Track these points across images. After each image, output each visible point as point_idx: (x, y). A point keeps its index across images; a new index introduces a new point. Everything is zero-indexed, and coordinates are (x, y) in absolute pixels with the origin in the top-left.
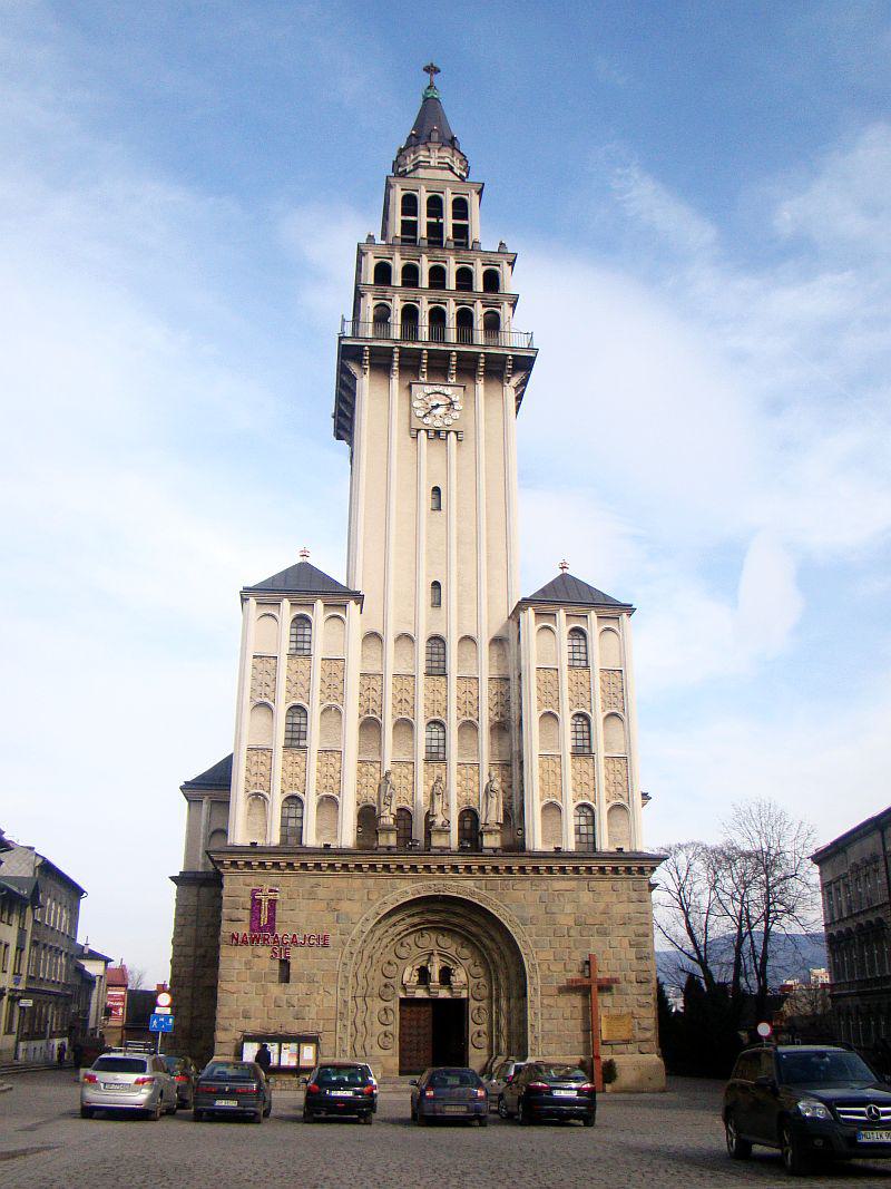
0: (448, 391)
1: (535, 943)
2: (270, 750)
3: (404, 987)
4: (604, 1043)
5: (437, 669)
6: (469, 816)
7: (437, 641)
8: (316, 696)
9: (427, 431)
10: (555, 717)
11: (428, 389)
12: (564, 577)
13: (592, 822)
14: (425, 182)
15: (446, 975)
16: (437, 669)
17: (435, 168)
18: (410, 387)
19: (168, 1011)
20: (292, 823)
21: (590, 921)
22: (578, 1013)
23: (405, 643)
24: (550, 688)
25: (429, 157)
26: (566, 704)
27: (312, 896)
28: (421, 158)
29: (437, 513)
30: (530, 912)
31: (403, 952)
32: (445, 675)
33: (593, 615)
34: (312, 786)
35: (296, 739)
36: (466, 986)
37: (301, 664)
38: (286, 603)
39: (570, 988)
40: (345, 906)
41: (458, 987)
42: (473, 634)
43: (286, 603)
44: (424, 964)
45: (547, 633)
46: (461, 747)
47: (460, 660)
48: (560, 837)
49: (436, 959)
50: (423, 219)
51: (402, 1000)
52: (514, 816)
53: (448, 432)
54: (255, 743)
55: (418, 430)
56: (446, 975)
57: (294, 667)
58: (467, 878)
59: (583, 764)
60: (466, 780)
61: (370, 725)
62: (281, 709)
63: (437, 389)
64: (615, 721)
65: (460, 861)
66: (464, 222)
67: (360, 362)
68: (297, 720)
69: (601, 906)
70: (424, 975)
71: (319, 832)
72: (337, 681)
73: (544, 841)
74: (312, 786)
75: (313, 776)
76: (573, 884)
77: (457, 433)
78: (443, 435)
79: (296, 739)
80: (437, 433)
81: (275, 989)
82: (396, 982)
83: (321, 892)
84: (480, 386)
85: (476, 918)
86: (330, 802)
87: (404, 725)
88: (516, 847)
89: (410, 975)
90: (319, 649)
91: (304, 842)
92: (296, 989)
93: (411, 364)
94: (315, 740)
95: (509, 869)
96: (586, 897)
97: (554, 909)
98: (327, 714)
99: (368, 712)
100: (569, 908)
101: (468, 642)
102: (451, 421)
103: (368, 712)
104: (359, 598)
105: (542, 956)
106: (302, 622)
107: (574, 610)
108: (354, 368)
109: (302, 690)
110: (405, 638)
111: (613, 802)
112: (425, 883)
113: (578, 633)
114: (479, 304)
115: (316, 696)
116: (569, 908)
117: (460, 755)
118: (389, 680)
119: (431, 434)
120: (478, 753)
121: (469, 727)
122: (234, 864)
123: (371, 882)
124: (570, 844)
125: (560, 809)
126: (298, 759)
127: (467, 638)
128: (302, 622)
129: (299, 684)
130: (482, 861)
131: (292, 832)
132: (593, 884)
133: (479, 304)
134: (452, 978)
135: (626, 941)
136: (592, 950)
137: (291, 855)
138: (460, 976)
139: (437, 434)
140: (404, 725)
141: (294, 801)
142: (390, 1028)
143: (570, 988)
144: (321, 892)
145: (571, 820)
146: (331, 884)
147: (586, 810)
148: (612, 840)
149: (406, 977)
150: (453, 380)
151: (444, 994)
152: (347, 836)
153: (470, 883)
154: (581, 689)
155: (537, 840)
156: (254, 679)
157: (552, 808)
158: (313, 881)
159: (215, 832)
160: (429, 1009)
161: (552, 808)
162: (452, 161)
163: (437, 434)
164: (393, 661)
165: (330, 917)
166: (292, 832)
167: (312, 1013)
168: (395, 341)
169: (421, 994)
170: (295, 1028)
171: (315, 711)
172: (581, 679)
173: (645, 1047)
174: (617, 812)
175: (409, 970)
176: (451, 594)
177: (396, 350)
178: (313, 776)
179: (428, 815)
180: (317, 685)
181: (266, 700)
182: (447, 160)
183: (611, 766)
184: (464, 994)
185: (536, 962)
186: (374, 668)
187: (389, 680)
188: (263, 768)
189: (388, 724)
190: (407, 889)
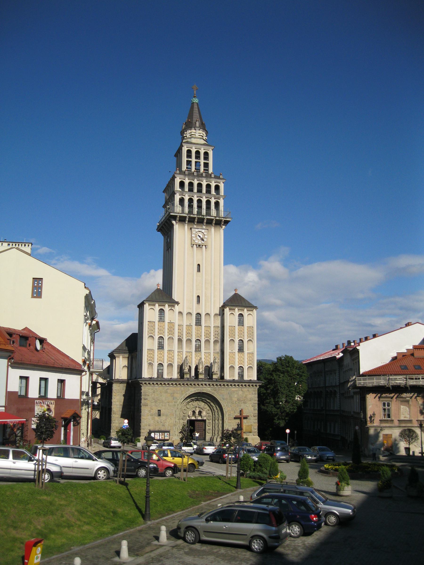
0: (203, 231)
1: (227, 405)
5: (198, 322)
7: (199, 314)
8: (166, 334)
9: (196, 245)
10: (234, 340)
11: (197, 230)
12: (235, 294)
13: (243, 371)
14: (194, 145)
15: (200, 413)
16: (198, 322)
17: (198, 138)
18: (191, 229)
19: (127, 424)
20: (160, 371)
21: (241, 399)
23: (189, 315)
24: (232, 332)
25: (195, 133)
26: (237, 336)
27: (166, 392)
28: (193, 133)
29: (199, 273)
31: (188, 406)
32: (201, 325)
33: (245, 310)
34: (166, 360)
35: (161, 347)
36: (205, 416)
37: (162, 324)
38: (157, 305)
40: (176, 395)
42: (209, 313)
43: (157, 305)
44: (194, 410)
45: (232, 315)
46: (205, 347)
47: (205, 321)
48: (234, 376)
53: (203, 245)
54: (149, 348)
56: (200, 413)
57: (160, 325)
59: (241, 355)
64: (250, 342)
65: (207, 383)
66: (207, 162)
68: (160, 341)
69: (244, 395)
70: (194, 412)
71: (168, 374)
73: (230, 377)
74: (166, 360)
75: (166, 358)
76: (237, 389)
77: (205, 246)
78: (201, 246)
79: (161, 347)
80: (199, 245)
81: (157, 418)
82: (186, 415)
83: (169, 391)
86: (170, 365)
87: (189, 341)
88: (222, 377)
89: (190, 413)
90: (167, 320)
91: (164, 377)
92: (163, 418)
93: (192, 220)
95: (220, 385)
96: (240, 393)
98: (169, 339)
100: (236, 396)
101: (208, 315)
104: (178, 303)
105: (228, 409)
106: (162, 311)
107: (240, 308)
108: (174, 222)
110: (189, 314)
111: (249, 366)
113: (241, 315)
114: (213, 198)
116: (236, 396)
117: (205, 350)
118: (185, 327)
119: (198, 246)
120: (209, 349)
121: (207, 341)
122: (145, 383)
123: (182, 388)
124: (236, 378)
125: (234, 368)
126: (161, 352)
127: (207, 314)
128: (162, 311)
129: (161, 330)
130: (213, 383)
131: (160, 374)
133: (213, 198)
135: (251, 406)
136: (242, 407)
137: (160, 380)
138: (204, 413)
140: (189, 341)
141: (161, 365)
144: (169, 391)
145: (237, 371)
146: (171, 389)
147: (241, 368)
148: (248, 376)
149: (189, 414)
151: (200, 418)
152: (175, 375)
153: (209, 389)
155: (227, 377)
156: (148, 328)
157: (232, 367)
158: (166, 388)
161: (232, 367)
164: (185, 321)
166: (160, 374)
167: (167, 424)
169: (193, 418)
170: (163, 429)
171: (166, 338)
172: (241, 329)
173: (255, 434)
175: (190, 412)
176: (202, 299)
178: (166, 358)
180: (166, 331)
181: (152, 335)
182: (202, 135)
183: (249, 355)
184: (205, 418)
185: (227, 411)
186: (181, 323)
187: (185, 327)
188: (151, 355)
190: (192, 390)
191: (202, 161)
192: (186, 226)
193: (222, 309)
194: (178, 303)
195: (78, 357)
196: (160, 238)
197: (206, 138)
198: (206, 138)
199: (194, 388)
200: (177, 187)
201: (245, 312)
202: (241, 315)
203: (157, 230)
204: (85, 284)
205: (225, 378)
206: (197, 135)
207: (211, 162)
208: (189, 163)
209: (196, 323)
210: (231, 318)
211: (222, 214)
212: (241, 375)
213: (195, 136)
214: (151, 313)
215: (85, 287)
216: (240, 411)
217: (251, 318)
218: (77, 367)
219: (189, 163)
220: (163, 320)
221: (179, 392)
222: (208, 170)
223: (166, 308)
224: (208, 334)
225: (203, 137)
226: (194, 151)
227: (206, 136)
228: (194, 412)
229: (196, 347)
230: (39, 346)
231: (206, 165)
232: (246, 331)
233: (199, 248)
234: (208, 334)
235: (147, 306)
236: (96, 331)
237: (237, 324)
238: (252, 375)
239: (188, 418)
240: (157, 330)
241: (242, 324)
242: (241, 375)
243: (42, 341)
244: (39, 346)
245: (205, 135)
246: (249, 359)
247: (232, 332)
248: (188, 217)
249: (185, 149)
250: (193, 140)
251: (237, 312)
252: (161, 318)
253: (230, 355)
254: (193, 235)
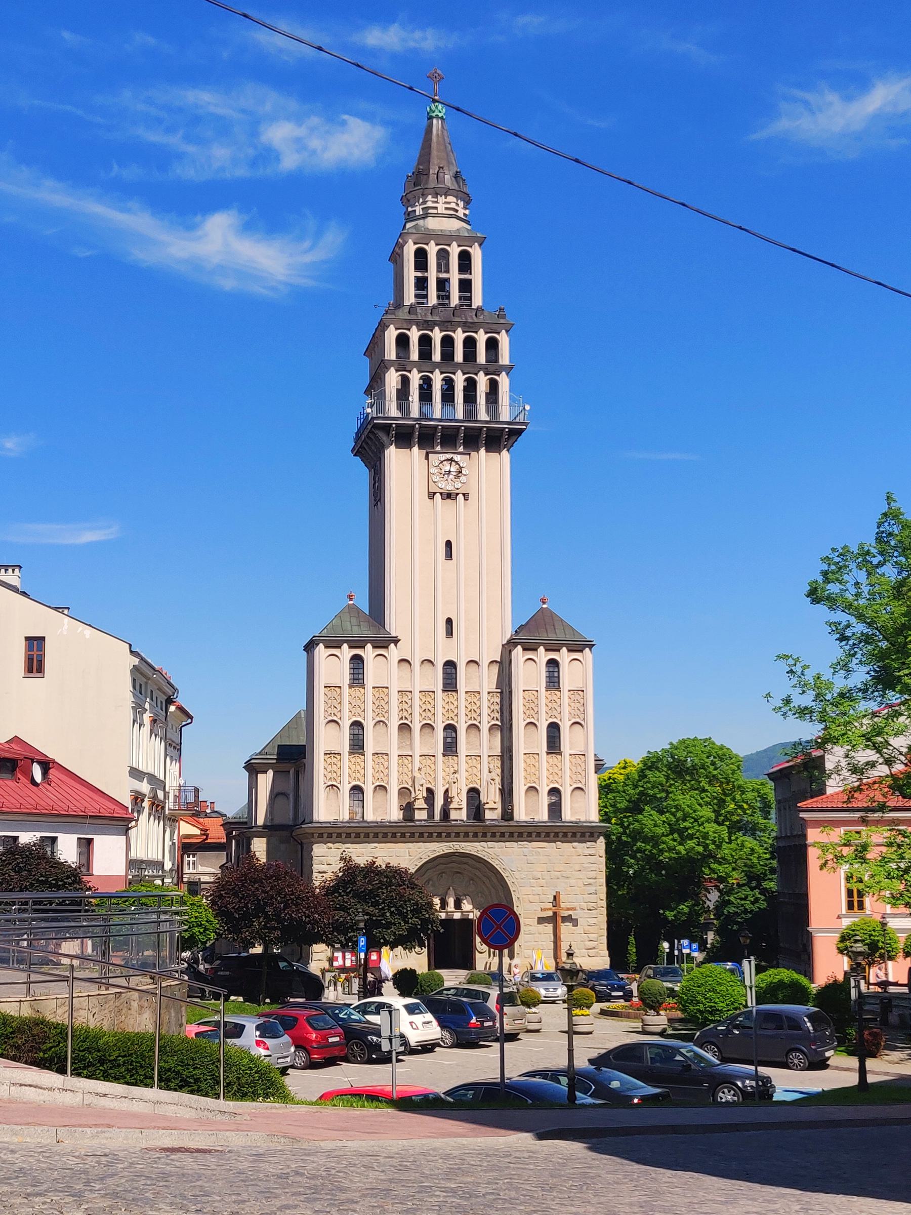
0: (457, 458)
2: (339, 754)
5: (450, 684)
6: (474, 793)
7: (450, 665)
8: (370, 714)
9: (441, 494)
10: (535, 725)
11: (443, 457)
16: (450, 684)
24: (532, 705)
25: (437, 202)
28: (430, 204)
32: (456, 691)
35: (357, 746)
37: (358, 691)
46: (467, 743)
50: (432, 274)
52: (507, 792)
53: (457, 494)
54: (329, 749)
55: (435, 493)
60: (472, 770)
61: (404, 728)
62: (346, 724)
63: (449, 456)
67: (388, 433)
68: (356, 732)
71: (375, 810)
72: (383, 703)
75: (370, 772)
77: (464, 495)
79: (357, 746)
84: (483, 451)
87: (428, 727)
88: (507, 814)
94: (370, 745)
98: (378, 727)
99: (402, 718)
102: (460, 485)
103: (402, 718)
104: (396, 641)
106: (357, 661)
109: (359, 710)
111: (575, 786)
113: (553, 663)
115: (370, 714)
118: (417, 695)
128: (357, 661)
139: (449, 496)
140: (428, 727)
145: (544, 800)
148: (573, 813)
150: (461, 449)
151: (457, 916)
154: (555, 705)
155: (521, 814)
159: (278, 794)
162: (457, 205)
163: (449, 496)
168: (416, 419)
171: (369, 725)
172: (555, 698)
174: (578, 792)
177: (417, 426)
178: (370, 772)
179: (447, 791)
180: (370, 707)
182: (453, 205)
187: (417, 695)
189: (416, 727)
191: (455, 277)
192: (416, 449)
193: (510, 645)
194: (396, 641)
195: (121, 790)
196: (361, 471)
197: (467, 212)
198: (467, 212)
200: (391, 352)
201: (564, 656)
202: (553, 663)
203: (352, 451)
204: (130, 645)
205: (516, 817)
206: (441, 209)
207: (477, 276)
208: (421, 283)
209: (445, 685)
210: (528, 671)
211: (505, 415)
212: (555, 809)
213: (435, 211)
214: (332, 666)
215: (131, 652)
216: (555, 897)
217: (576, 670)
218: (120, 813)
219: (421, 283)
220: (361, 681)
222: (470, 298)
223: (368, 653)
224: (474, 711)
225: (457, 211)
226: (432, 250)
227: (465, 208)
229: (445, 743)
230: (38, 777)
231: (465, 286)
232: (566, 700)
233: (448, 500)
234: (474, 711)
235: (321, 651)
236: (184, 723)
237: (544, 684)
238: (584, 809)
240: (346, 707)
241: (556, 684)
242: (555, 809)
243: (47, 765)
244: (38, 777)
245: (461, 204)
246: (574, 769)
247: (532, 705)
248: (417, 426)
249: (410, 250)
250: (432, 224)
251: (542, 656)
252: (356, 676)
253: (528, 761)
254: (432, 471)
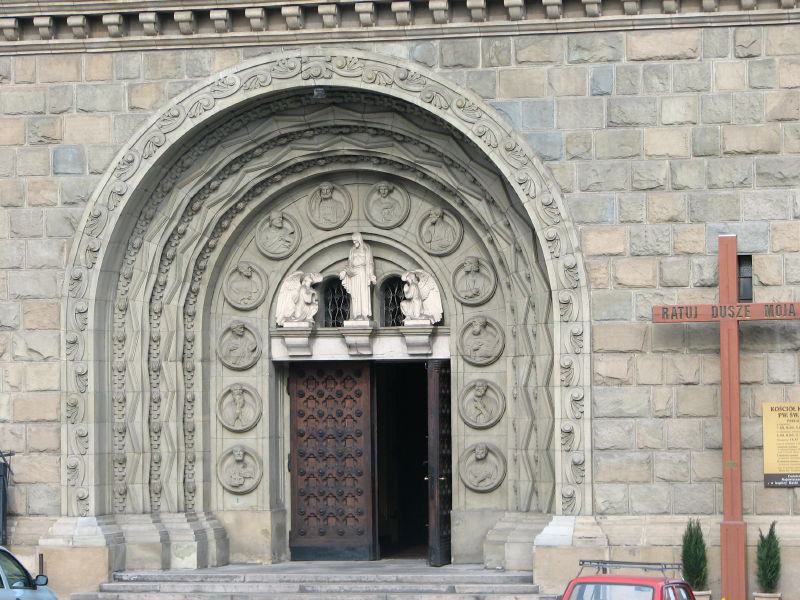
3: (281, 332)
4: (771, 481)
15: (391, 291)
21: (736, 141)
22: (702, 400)
30: (565, 124)
36: (437, 328)
39: (680, 331)
41: (416, 331)
49: (361, 257)
51: (279, 367)
58: (388, 38)
70: (333, 299)
76: (688, 39)
85: (440, 144)
89: (295, 302)
96: (728, 74)
97: (639, 112)
100: (675, 109)
105: (597, 242)
112: (279, 55)
116: (675, 109)
123: (137, 61)
132: (746, 35)
134: (405, 307)
138: (424, 302)
142: (248, 440)
143: (680, 331)
151: (390, 349)
153: (400, 50)
160: (364, 386)
165: (36, 160)
169: (329, 349)
184: (442, 350)
190: (228, 76)
199: (252, 47)
221: (102, 103)
228: (333, 299)
239: (280, 354)
